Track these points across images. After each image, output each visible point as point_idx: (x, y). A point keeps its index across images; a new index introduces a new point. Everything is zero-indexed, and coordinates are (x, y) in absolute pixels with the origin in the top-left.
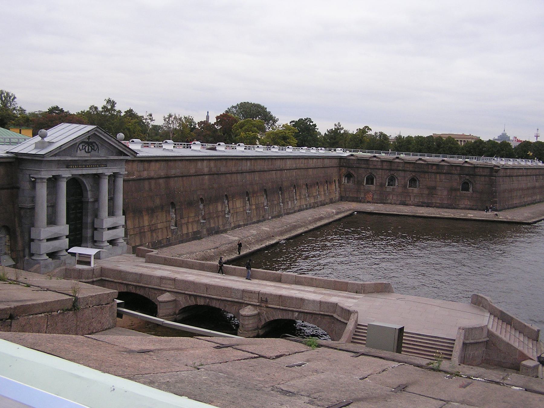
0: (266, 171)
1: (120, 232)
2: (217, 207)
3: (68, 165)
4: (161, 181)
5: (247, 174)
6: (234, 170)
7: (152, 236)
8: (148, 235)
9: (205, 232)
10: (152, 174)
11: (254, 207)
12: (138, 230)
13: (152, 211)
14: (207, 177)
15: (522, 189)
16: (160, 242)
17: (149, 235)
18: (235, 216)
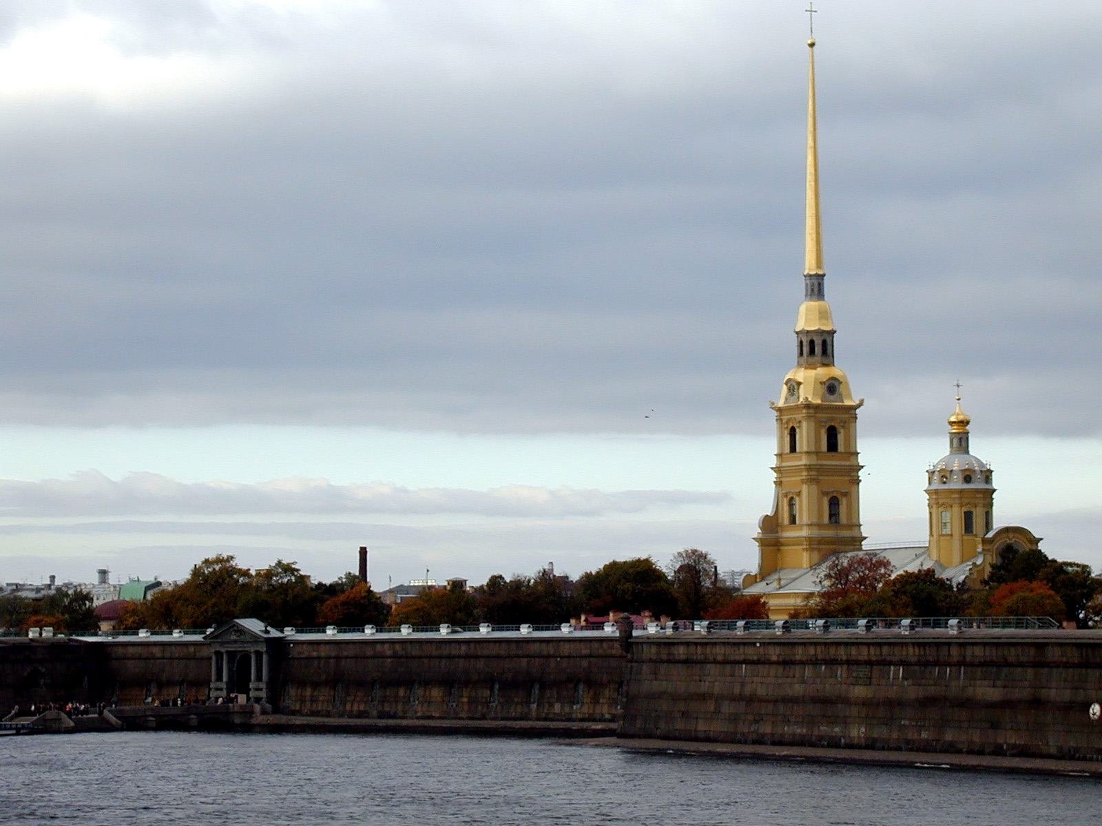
0: (501, 657)
1: (263, 694)
2: (397, 692)
3: (222, 644)
4: (331, 661)
5: (462, 661)
6: (434, 653)
7: (311, 704)
8: (308, 704)
9: (375, 713)
10: (323, 654)
11: (465, 700)
12: (299, 697)
13: (316, 685)
14: (389, 660)
15: (751, 700)
16: (319, 712)
17: (309, 704)
18: (425, 705)
